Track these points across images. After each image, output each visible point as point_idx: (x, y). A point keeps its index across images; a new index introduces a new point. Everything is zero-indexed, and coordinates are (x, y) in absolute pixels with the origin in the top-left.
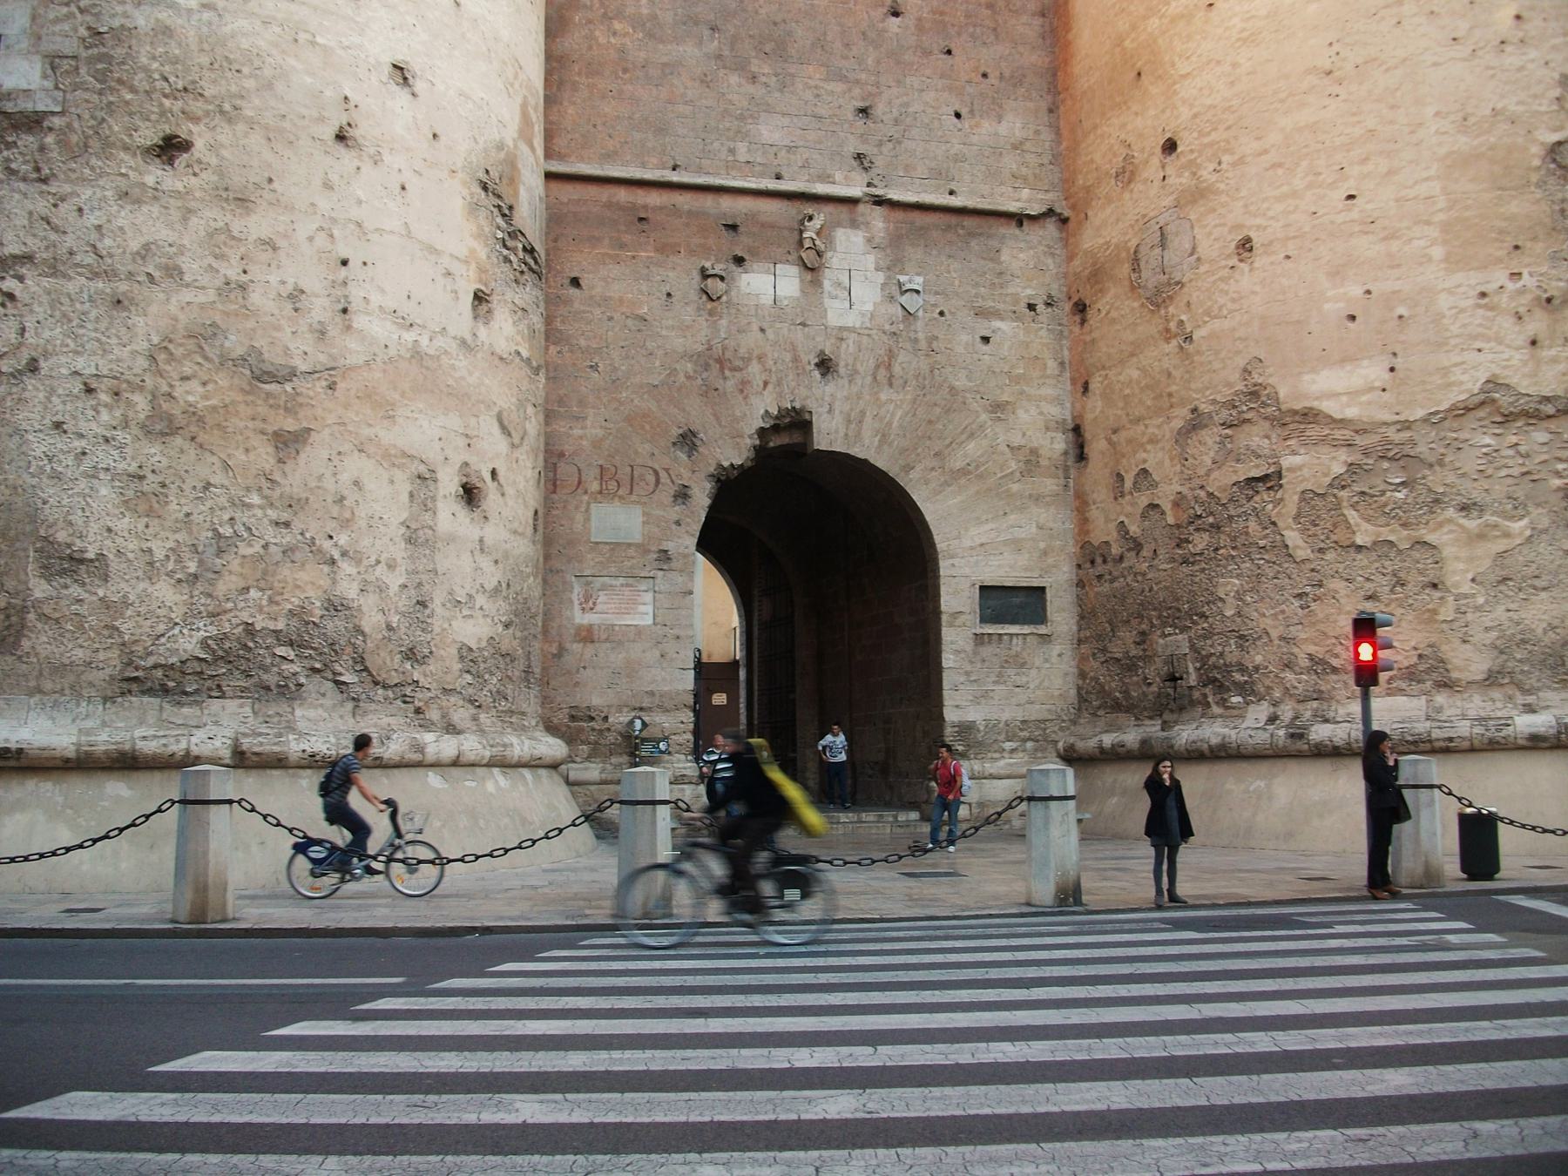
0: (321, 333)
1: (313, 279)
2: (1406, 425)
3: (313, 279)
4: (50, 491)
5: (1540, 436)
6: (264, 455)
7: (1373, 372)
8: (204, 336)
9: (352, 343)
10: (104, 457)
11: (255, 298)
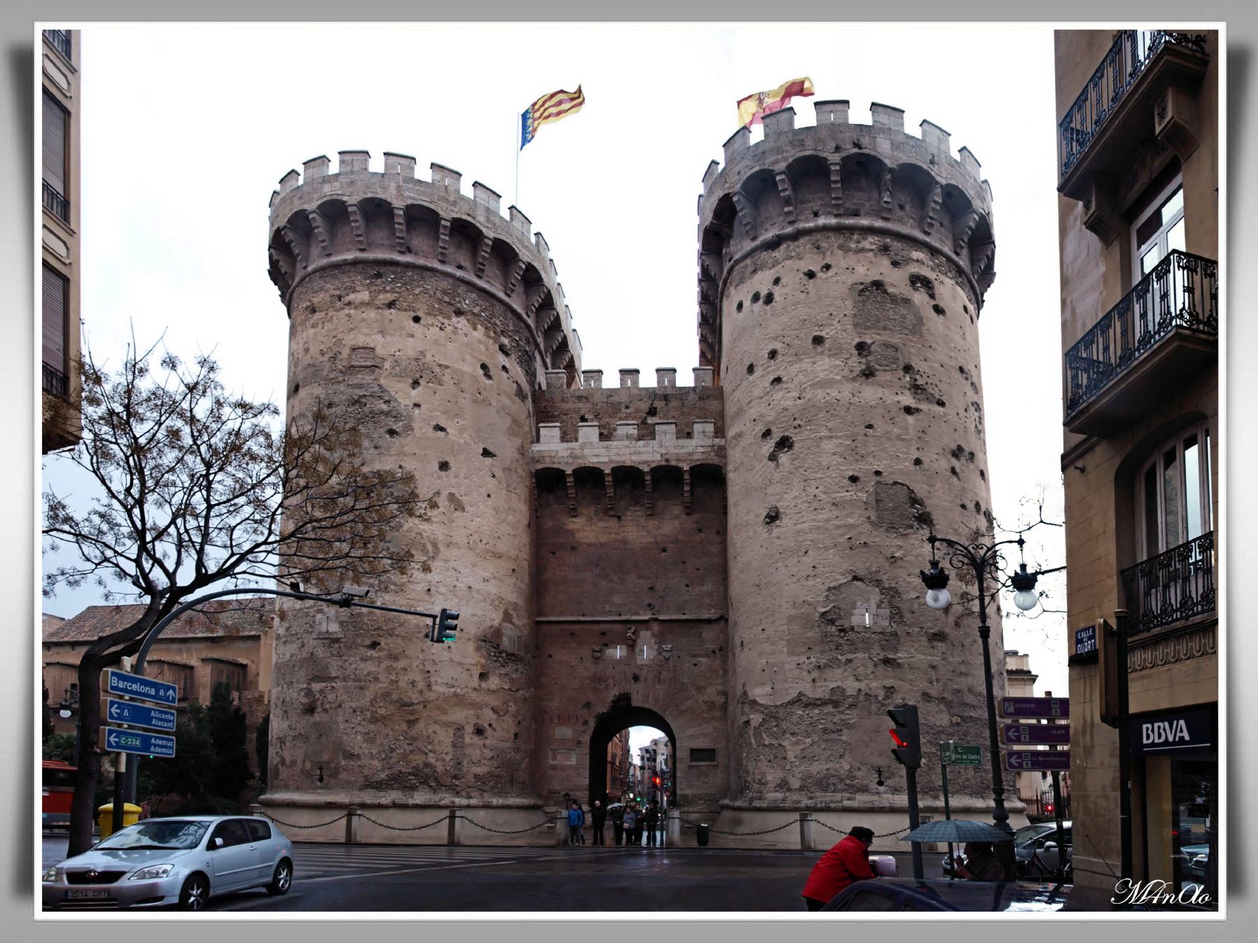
0: (421, 692)
1: (418, 678)
2: (776, 707)
3: (418, 678)
4: (345, 738)
5: (817, 711)
6: (404, 726)
7: (768, 689)
8: (386, 695)
9: (432, 694)
10: (360, 729)
11: (401, 684)
